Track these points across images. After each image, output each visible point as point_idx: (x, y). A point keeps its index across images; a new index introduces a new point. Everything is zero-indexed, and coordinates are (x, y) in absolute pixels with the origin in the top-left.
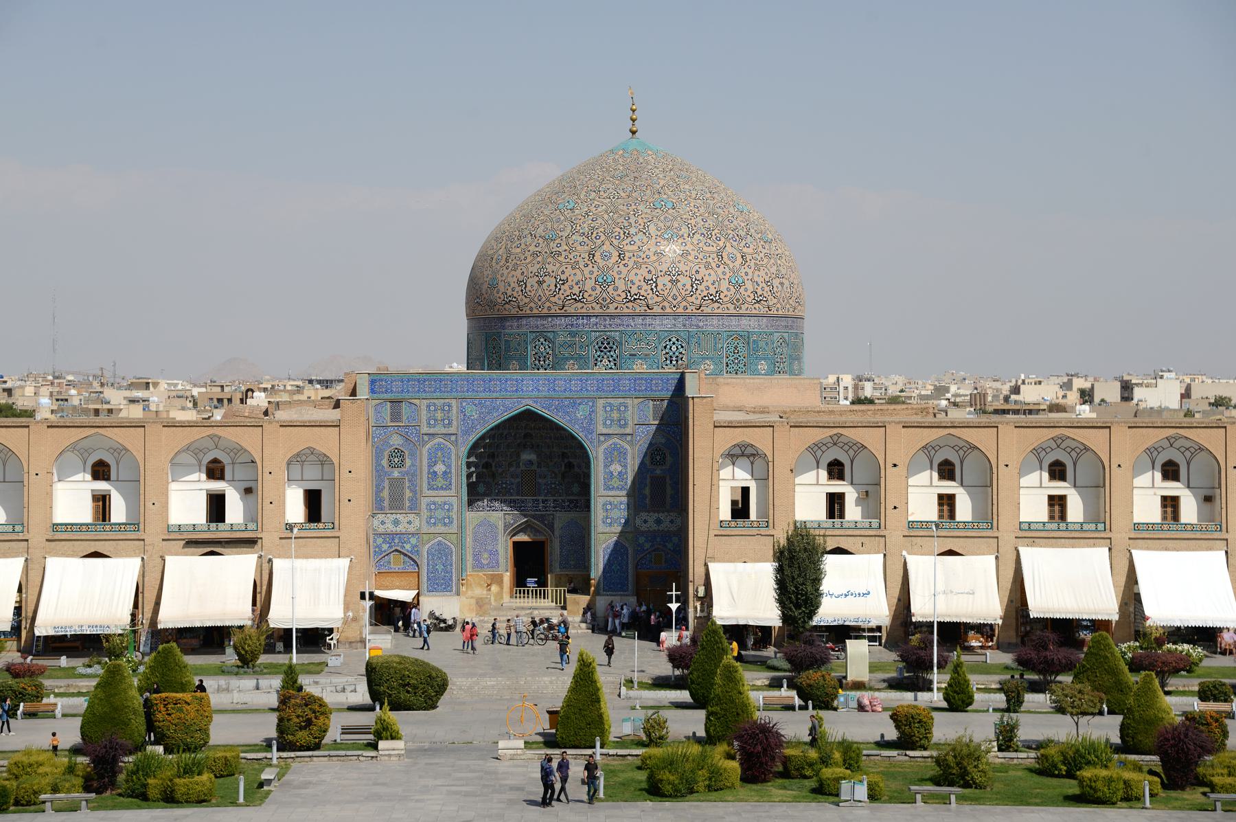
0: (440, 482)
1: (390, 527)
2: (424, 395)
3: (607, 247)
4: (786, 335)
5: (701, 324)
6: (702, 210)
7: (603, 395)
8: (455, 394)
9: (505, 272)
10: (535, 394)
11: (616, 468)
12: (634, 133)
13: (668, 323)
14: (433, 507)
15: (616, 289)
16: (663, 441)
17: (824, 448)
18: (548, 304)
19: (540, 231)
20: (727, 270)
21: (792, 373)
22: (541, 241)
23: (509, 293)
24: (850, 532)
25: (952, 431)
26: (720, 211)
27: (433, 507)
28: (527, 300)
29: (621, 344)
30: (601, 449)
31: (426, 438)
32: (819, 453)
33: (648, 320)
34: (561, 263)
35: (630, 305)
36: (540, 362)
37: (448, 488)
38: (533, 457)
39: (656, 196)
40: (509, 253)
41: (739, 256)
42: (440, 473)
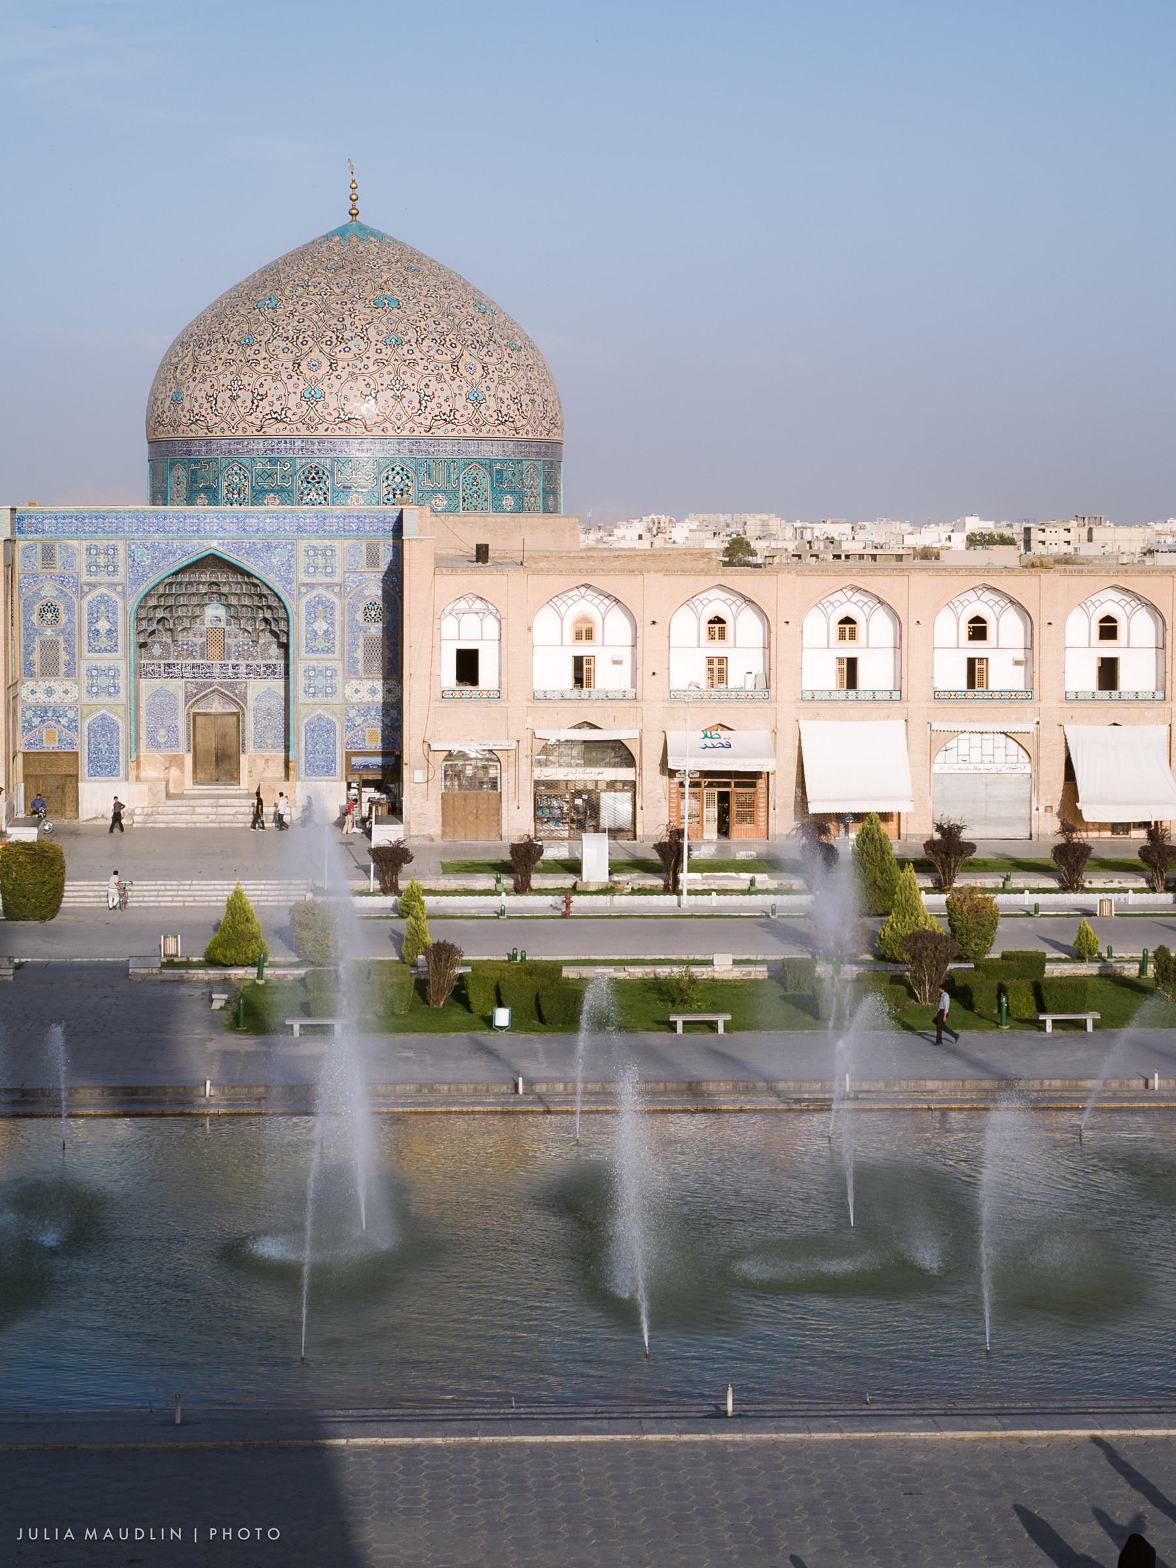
0: (104, 642)
1: (42, 697)
3: (316, 354)
6: (434, 310)
11: (321, 626)
14: (94, 673)
15: (326, 406)
17: (569, 602)
18: (243, 424)
19: (235, 335)
20: (464, 383)
21: (546, 510)
22: (235, 346)
26: (457, 311)
27: (94, 673)
28: (217, 420)
29: (332, 473)
30: (304, 600)
31: (86, 589)
32: (563, 608)
34: (258, 373)
35: (343, 425)
36: (236, 496)
37: (113, 649)
39: (378, 293)
40: (196, 359)
41: (479, 366)
42: (103, 632)
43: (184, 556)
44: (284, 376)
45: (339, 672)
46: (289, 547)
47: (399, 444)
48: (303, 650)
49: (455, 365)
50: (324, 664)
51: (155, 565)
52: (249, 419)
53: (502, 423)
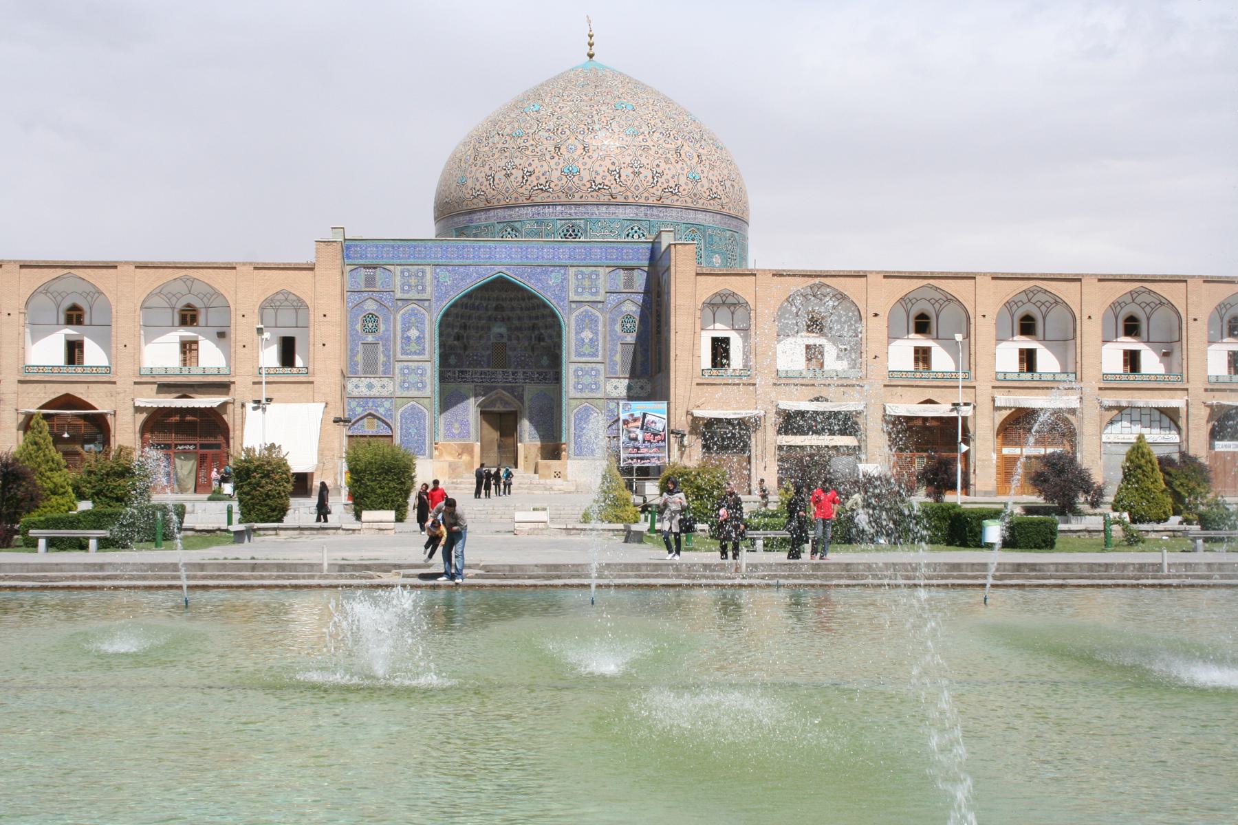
0: (414, 347)
1: (364, 391)
2: (398, 262)
6: (660, 114)
8: (429, 261)
10: (508, 261)
11: (587, 335)
12: (591, 56)
13: (630, 213)
14: (406, 371)
25: (932, 282)
27: (406, 371)
28: (495, 193)
33: (612, 209)
35: (594, 194)
37: (421, 352)
38: (503, 330)
41: (695, 155)
45: (602, 372)
48: (573, 354)
52: (520, 190)
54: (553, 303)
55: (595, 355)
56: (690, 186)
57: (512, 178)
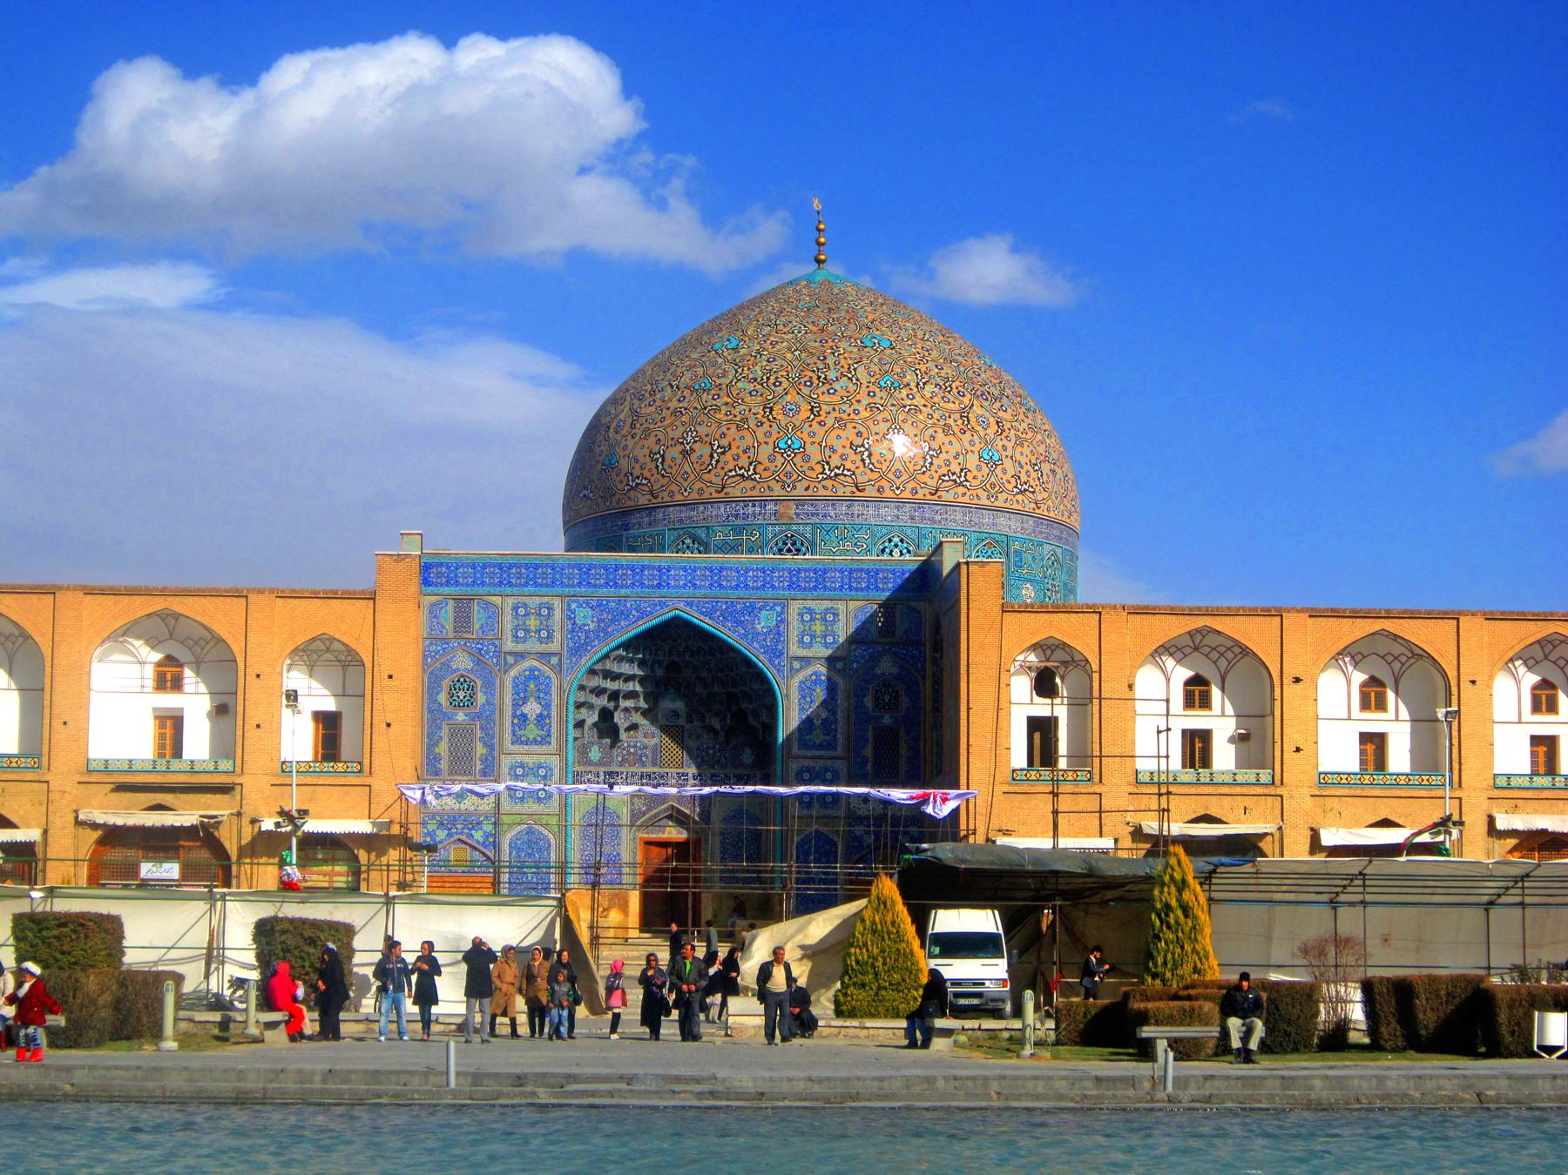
0: (532, 731)
1: (450, 803)
4: (1059, 551)
5: (938, 518)
6: (934, 354)
7: (799, 594)
9: (630, 443)
13: (888, 512)
15: (806, 459)
16: (895, 671)
18: (698, 485)
19: (686, 380)
23: (637, 472)
24: (1225, 790)
25: (1388, 625)
29: (813, 544)
31: (511, 660)
33: (857, 509)
34: (719, 423)
35: (828, 483)
37: (545, 740)
39: (865, 331)
40: (635, 413)
42: (532, 716)
43: (639, 619)
44: (752, 423)
46: (778, 609)
47: (898, 508)
49: (964, 414)
50: (822, 762)
51: (602, 631)
52: (706, 477)
53: (1022, 492)
54: (761, 661)
55: (831, 746)
56: (985, 470)
57: (694, 457)
